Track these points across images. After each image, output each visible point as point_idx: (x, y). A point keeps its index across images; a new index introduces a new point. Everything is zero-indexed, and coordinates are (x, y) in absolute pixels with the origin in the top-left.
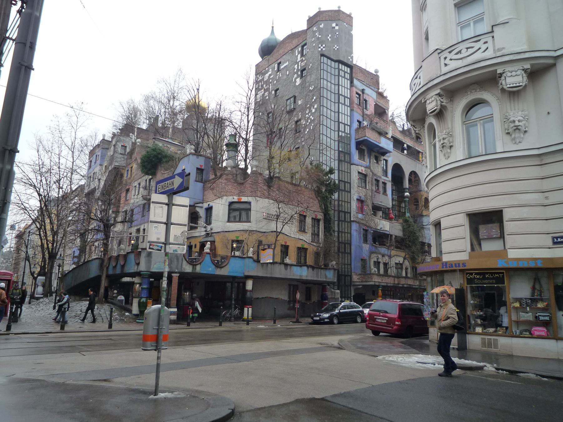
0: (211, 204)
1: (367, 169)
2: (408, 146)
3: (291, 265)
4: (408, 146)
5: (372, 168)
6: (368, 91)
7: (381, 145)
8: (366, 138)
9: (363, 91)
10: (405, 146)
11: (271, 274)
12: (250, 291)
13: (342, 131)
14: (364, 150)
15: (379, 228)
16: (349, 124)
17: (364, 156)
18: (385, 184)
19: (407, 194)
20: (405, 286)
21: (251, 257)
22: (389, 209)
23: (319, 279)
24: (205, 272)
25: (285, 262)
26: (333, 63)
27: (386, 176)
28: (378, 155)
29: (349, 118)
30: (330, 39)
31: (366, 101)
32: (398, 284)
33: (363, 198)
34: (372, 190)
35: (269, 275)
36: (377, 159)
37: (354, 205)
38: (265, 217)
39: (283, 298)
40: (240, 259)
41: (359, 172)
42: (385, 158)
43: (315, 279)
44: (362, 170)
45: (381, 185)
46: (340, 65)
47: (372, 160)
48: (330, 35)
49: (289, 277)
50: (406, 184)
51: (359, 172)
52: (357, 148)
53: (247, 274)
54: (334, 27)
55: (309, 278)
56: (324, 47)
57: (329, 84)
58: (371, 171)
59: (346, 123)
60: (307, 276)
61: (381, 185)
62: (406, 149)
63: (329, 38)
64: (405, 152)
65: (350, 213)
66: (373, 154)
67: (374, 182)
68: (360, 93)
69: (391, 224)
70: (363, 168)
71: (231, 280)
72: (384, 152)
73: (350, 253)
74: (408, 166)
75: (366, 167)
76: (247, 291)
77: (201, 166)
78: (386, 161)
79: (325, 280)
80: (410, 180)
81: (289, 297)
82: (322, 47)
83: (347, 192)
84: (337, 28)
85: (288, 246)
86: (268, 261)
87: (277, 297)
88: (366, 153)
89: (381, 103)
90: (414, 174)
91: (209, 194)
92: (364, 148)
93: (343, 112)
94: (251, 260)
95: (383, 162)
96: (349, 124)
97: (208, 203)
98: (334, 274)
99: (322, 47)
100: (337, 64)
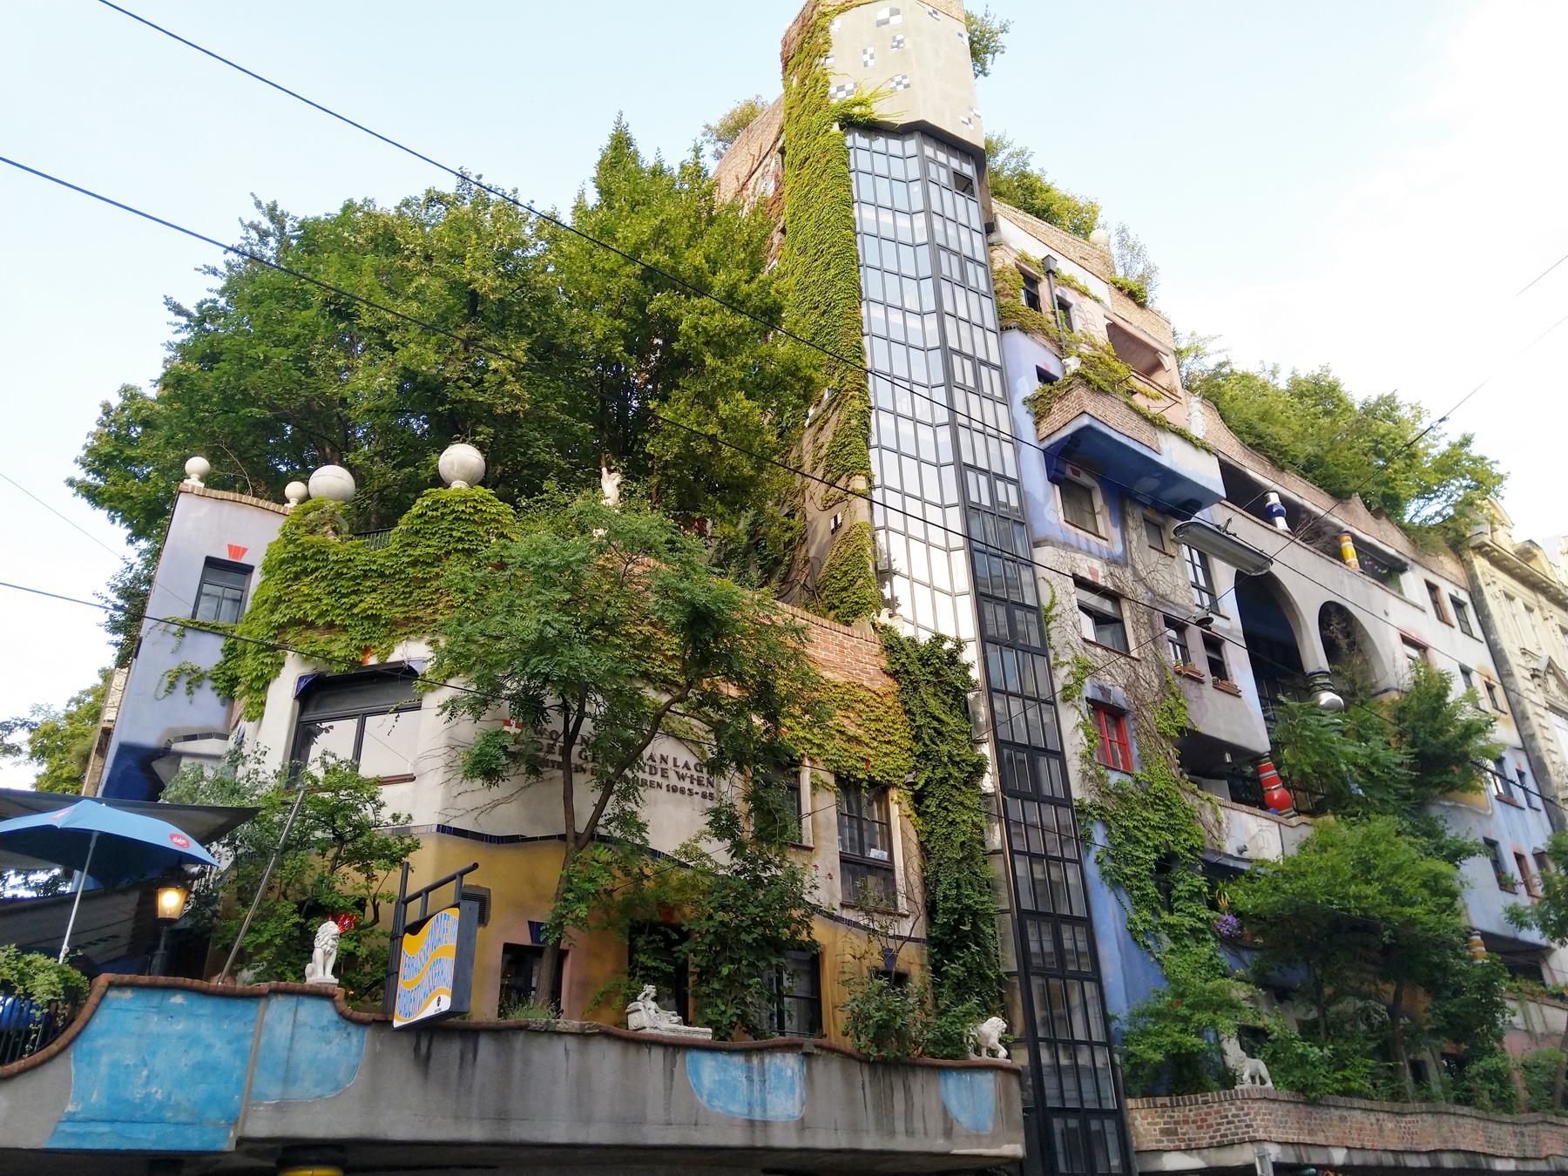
1: (1118, 571)
3: (674, 1047)
5: (1140, 567)
7: (1164, 460)
8: (1085, 421)
10: (1274, 499)
11: (502, 1117)
13: (963, 388)
15: (1230, 848)
17: (1093, 514)
19: (1326, 698)
20: (1448, 1162)
21: (320, 994)
22: (1255, 758)
23: (901, 1143)
25: (634, 1021)
26: (895, 145)
30: (871, 63)
31: (1064, 306)
33: (1119, 696)
34: (1162, 667)
35: (475, 1132)
36: (1155, 529)
37: (1073, 730)
40: (206, 1007)
41: (1075, 576)
43: (870, 1142)
44: (1093, 572)
46: (929, 151)
47: (1134, 536)
48: (870, 50)
49: (655, 1136)
50: (1314, 655)
51: (1080, 583)
52: (1054, 477)
53: (261, 1126)
54: (886, 22)
55: (824, 1139)
56: (849, 93)
57: (886, 217)
58: (1140, 580)
59: (981, 355)
60: (802, 1125)
62: (1279, 513)
63: (866, 58)
64: (1281, 522)
65: (1060, 755)
67: (1160, 624)
69: (1287, 831)
70: (1096, 564)
73: (1096, 977)
74: (1308, 582)
75: (1112, 561)
77: (237, 550)
79: (939, 1145)
82: (842, 95)
83: (1027, 649)
84: (895, 20)
86: (430, 1010)
88: (1098, 501)
89: (1135, 322)
90: (1335, 617)
92: (1085, 479)
93: (962, 313)
94: (326, 1012)
96: (995, 360)
98: (1004, 1095)
99: (842, 95)
100: (911, 145)
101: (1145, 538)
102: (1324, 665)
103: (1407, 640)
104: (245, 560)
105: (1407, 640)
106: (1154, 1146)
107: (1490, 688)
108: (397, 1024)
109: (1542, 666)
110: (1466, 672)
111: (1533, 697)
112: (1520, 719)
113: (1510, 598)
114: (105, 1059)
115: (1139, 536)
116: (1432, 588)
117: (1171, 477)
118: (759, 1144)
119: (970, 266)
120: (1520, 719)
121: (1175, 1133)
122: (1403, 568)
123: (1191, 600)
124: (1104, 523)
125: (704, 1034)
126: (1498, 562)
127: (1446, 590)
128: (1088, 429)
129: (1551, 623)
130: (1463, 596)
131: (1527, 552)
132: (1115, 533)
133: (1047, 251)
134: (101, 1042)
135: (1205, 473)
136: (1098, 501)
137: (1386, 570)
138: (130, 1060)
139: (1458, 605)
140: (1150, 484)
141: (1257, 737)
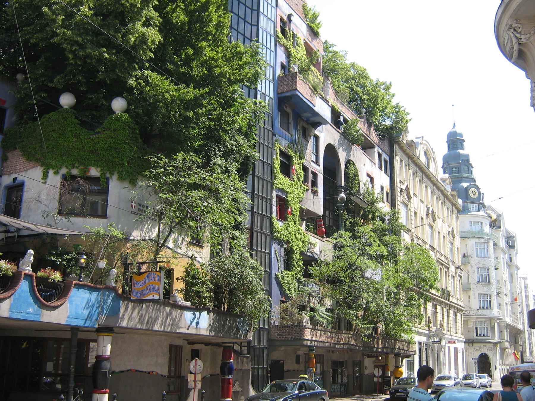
0: (20, 178)
2: (344, 118)
4: (344, 118)
6: (295, 19)
7: (316, 109)
8: (297, 92)
9: (289, 16)
12: (107, 359)
14: (288, 114)
16: (272, 64)
18: (315, 175)
24: (18, 316)
27: (317, 162)
28: (306, 126)
29: (272, 54)
32: (337, 344)
38: (134, 209)
39: (159, 372)
42: (316, 132)
45: (310, 176)
61: (310, 176)
66: (302, 123)
68: (285, 18)
71: (68, 335)
72: (316, 121)
76: (100, 359)
78: (317, 138)
80: (346, 174)
81: (170, 371)
85: (173, 270)
86: (150, 297)
87: (149, 370)
88: (291, 120)
91: (16, 158)
92: (288, 110)
95: (312, 140)
97: (14, 176)
101: (302, 134)
102: (343, 184)
103: (368, 175)
104: (6, 106)
105: (368, 175)
106: (275, 338)
107: (387, 193)
108: (132, 298)
109: (404, 187)
110: (382, 188)
111: (400, 198)
112: (393, 205)
113: (401, 161)
114: (74, 303)
115: (300, 133)
116: (380, 155)
117: (316, 114)
118: (198, 333)
119: (269, 22)
120: (393, 205)
121: (282, 335)
122: (373, 147)
123: (311, 158)
124: (292, 126)
125: (189, 304)
126: (401, 148)
127: (384, 156)
128: (297, 95)
129: (411, 171)
130: (388, 159)
131: (412, 144)
132: (293, 132)
133: (291, 12)
134: (73, 298)
135: (325, 112)
136: (291, 120)
137: (367, 147)
138: (79, 303)
139: (385, 161)
140: (308, 115)
141: (320, 211)
